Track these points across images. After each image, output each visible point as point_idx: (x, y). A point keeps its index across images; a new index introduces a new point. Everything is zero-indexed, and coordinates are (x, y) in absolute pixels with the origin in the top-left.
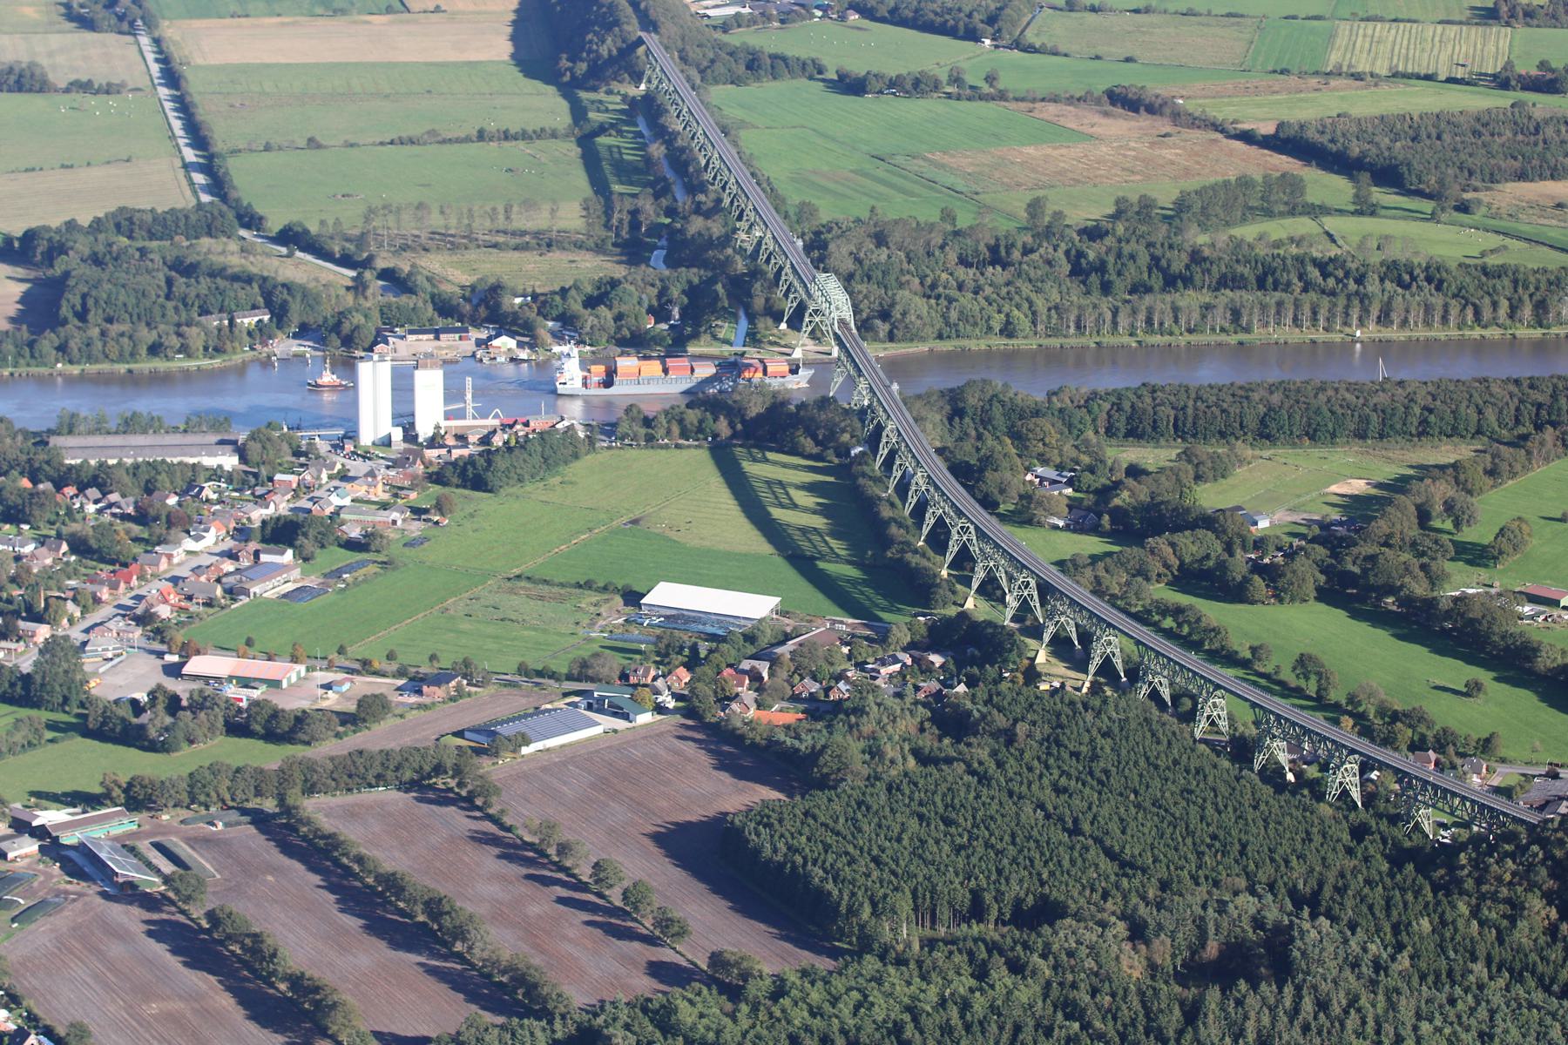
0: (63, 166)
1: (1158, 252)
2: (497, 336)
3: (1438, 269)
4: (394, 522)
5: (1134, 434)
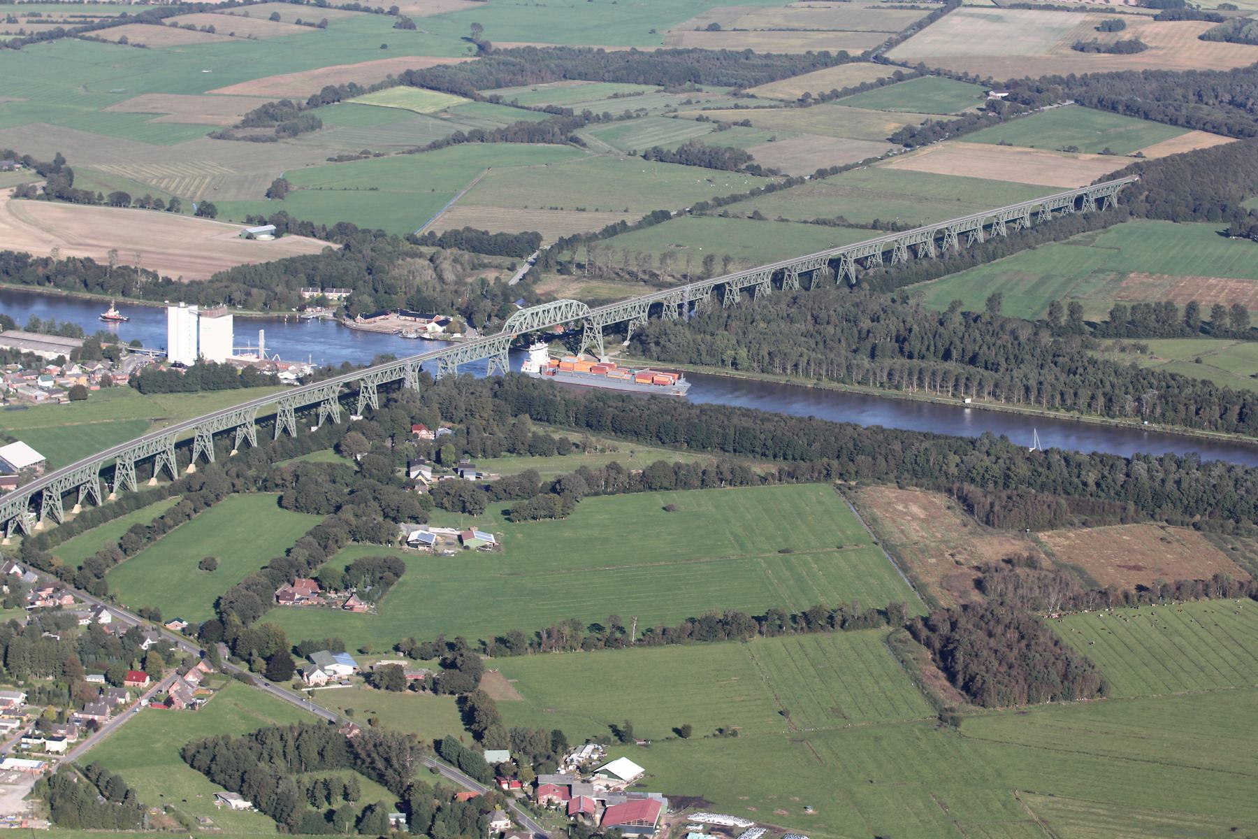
0: (577, 209)
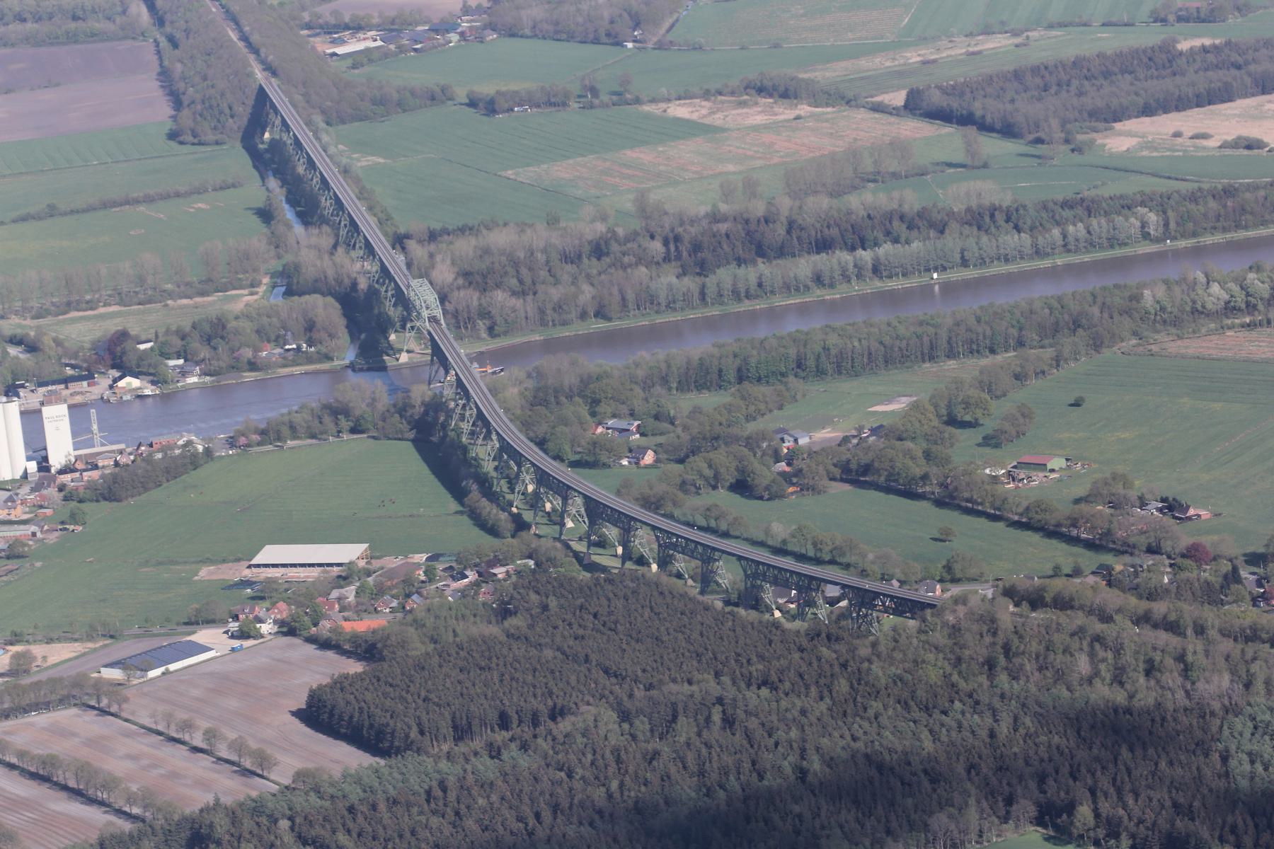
1: (753, 227)
2: (121, 378)
3: (1017, 210)
4: (34, 534)
5: (701, 386)
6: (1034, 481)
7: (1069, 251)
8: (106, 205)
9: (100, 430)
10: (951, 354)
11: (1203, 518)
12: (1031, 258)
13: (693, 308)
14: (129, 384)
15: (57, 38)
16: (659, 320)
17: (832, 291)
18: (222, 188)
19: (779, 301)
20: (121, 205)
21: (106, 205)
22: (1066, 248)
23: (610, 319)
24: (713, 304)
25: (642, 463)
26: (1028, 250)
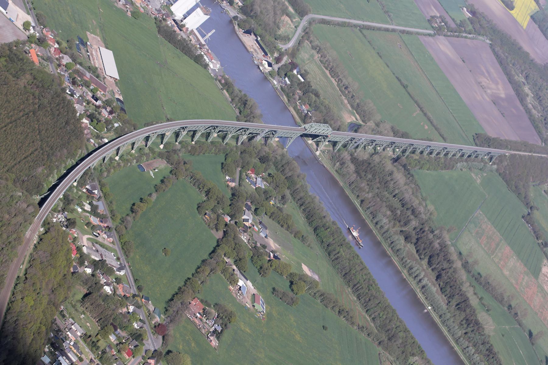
6: (240, 297)
7: (463, 351)
8: (416, 102)
9: (209, 37)
10: (358, 297)
11: (211, 343)
12: (454, 339)
13: (379, 232)
14: (265, 64)
15: (534, 123)
16: (368, 221)
17: (408, 276)
18: (440, 135)
19: (395, 260)
20: (419, 107)
21: (416, 102)
22: (463, 350)
23: (361, 206)
24: (383, 238)
25: (228, 183)
26: (456, 336)
